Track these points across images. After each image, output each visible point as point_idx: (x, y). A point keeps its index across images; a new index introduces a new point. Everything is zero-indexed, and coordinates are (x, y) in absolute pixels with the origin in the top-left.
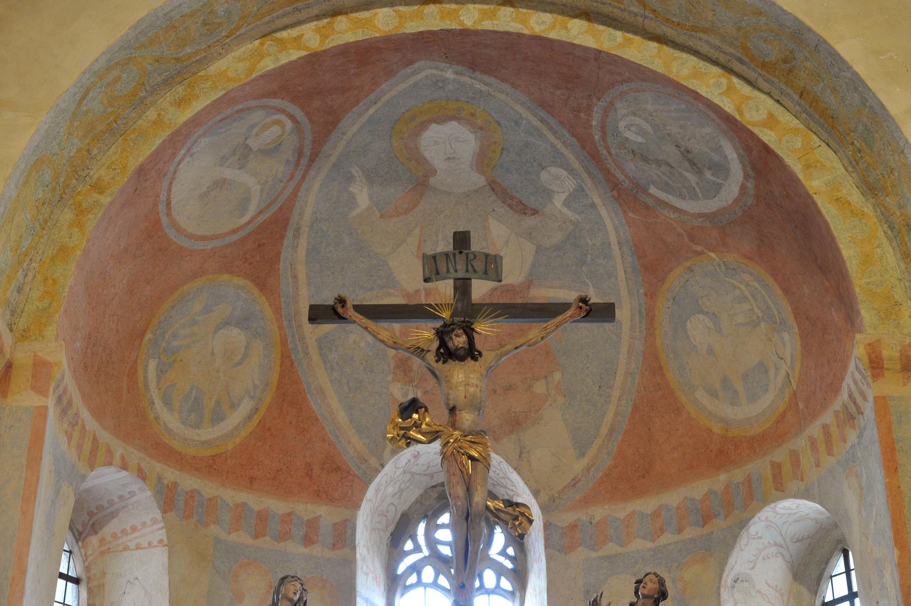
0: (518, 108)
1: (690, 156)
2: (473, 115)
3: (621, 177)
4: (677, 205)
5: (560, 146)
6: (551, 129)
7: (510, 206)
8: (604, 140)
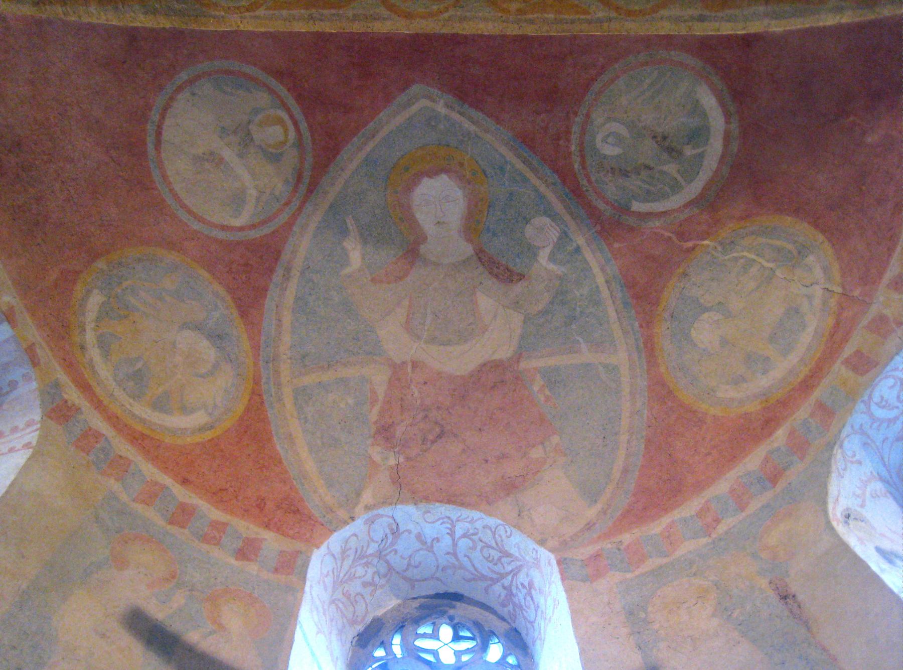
0: (503, 150)
1: (667, 143)
2: (461, 165)
3: (601, 206)
4: (662, 209)
5: (542, 188)
6: (534, 170)
7: (497, 276)
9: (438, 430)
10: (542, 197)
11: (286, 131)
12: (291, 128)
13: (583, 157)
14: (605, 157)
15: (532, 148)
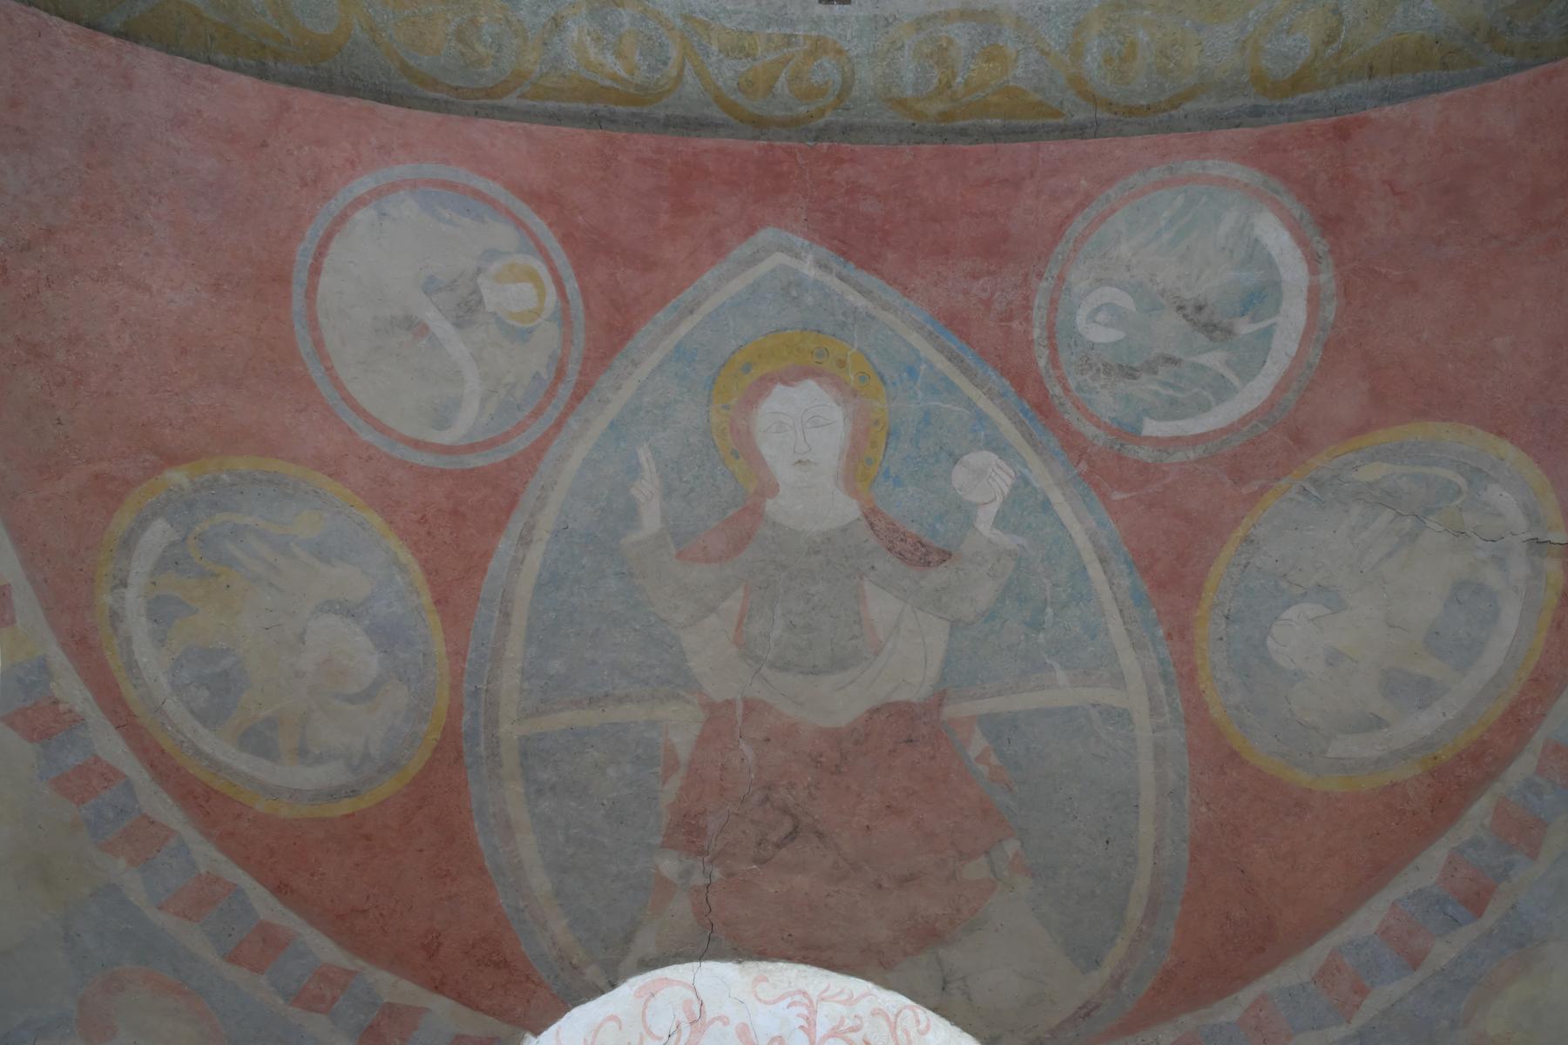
0: (915, 339)
2: (842, 364)
3: (1089, 430)
4: (1198, 430)
5: (983, 403)
6: (966, 371)
7: (901, 556)
8: (1054, 361)
9: (787, 825)
10: (981, 417)
11: (542, 294)
12: (551, 290)
13: (1053, 348)
14: (1093, 346)
15: (964, 336)
